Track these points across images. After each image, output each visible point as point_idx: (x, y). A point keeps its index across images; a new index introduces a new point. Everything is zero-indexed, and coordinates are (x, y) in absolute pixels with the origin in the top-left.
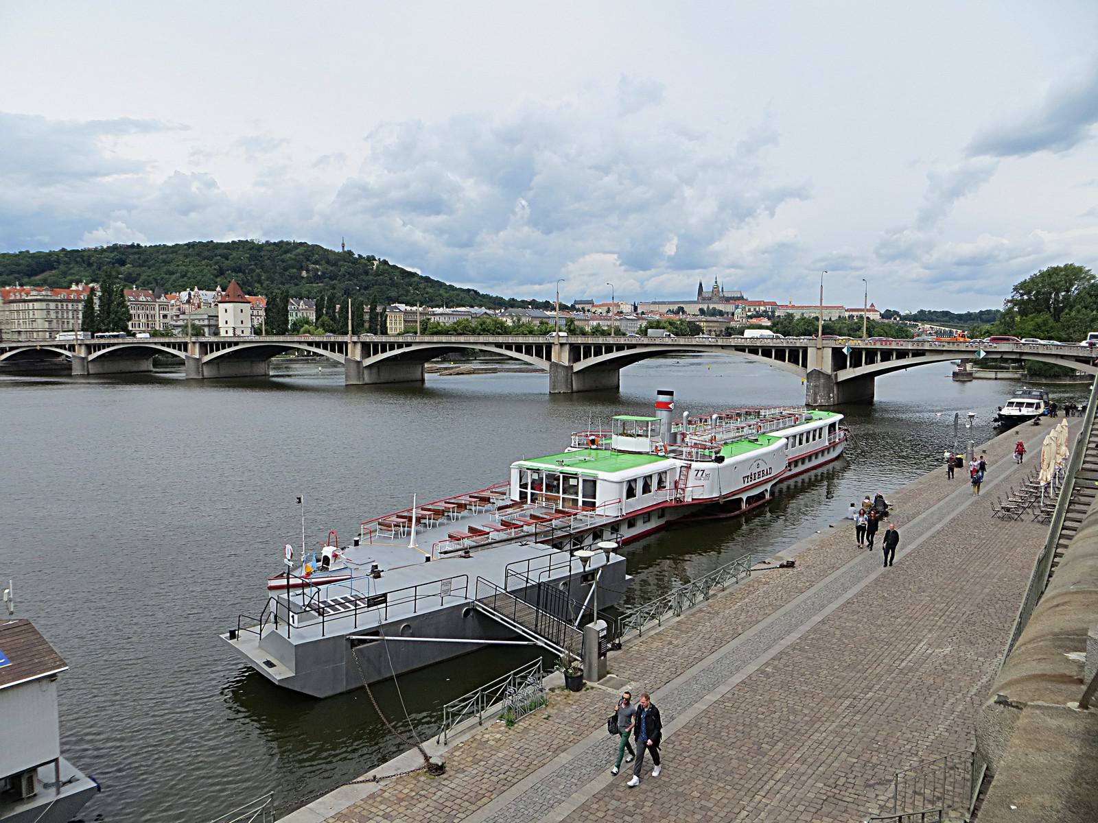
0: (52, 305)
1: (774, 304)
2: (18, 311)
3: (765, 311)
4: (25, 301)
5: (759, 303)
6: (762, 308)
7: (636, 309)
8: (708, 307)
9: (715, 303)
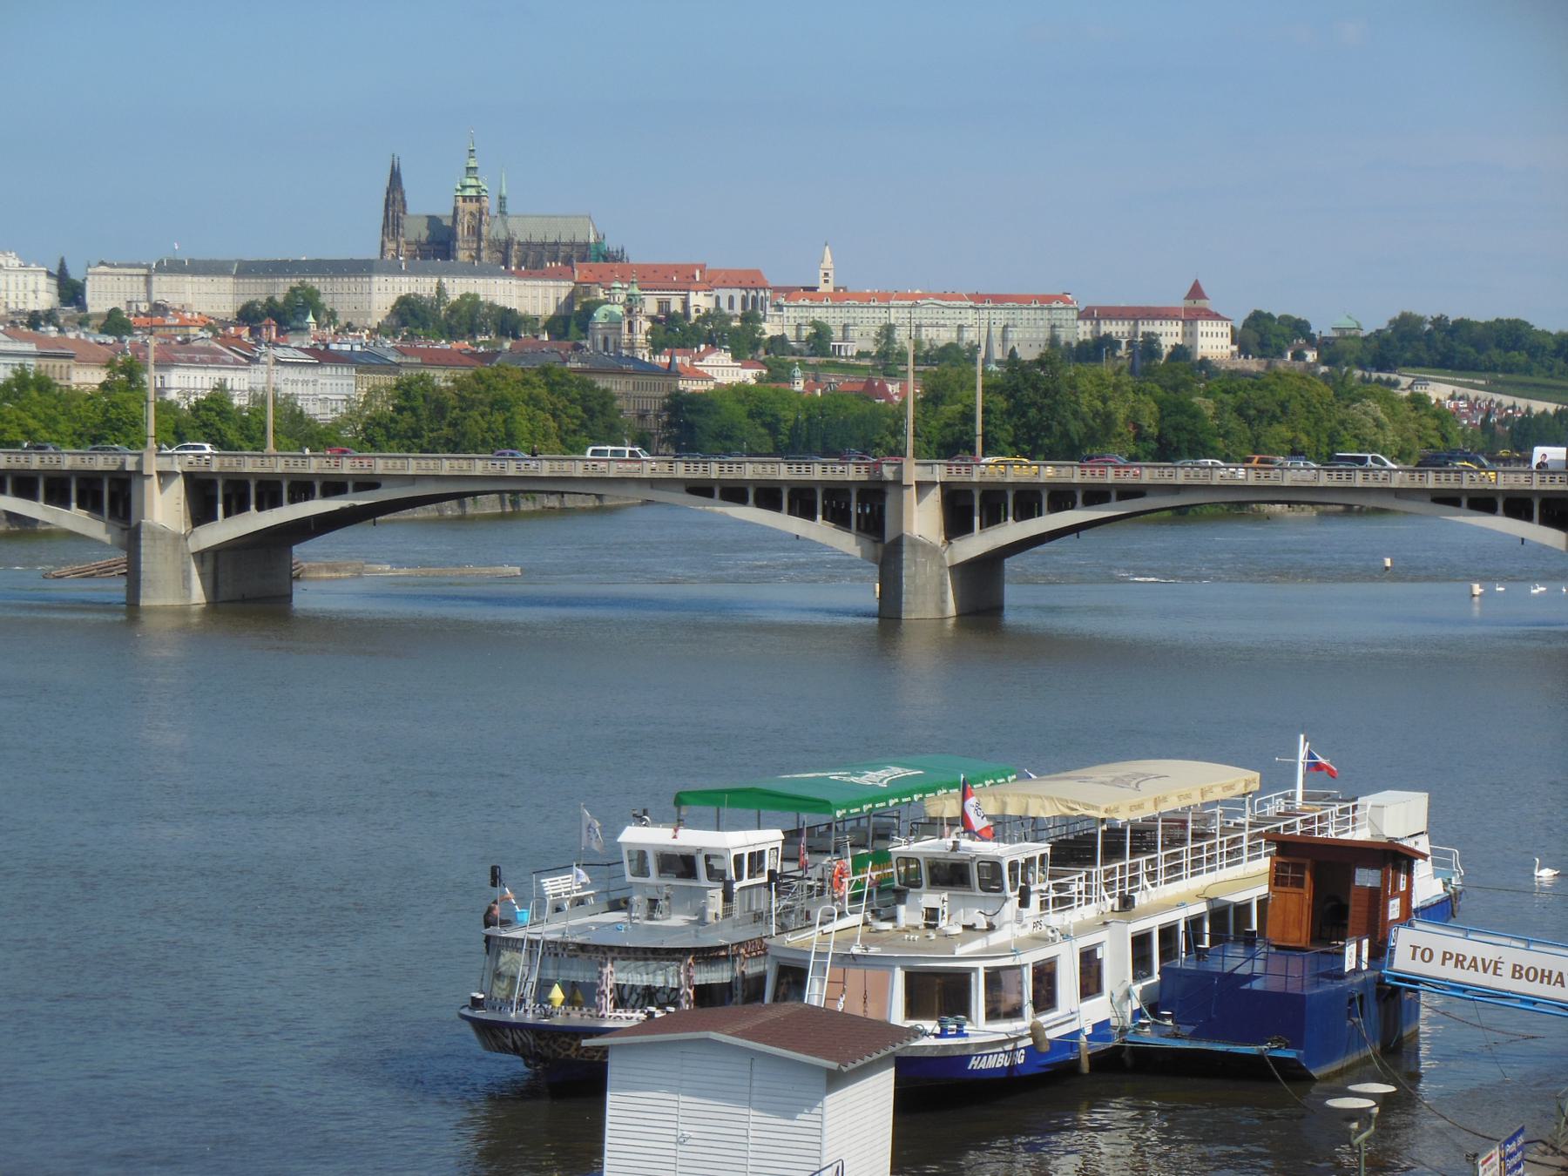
1: (750, 281)
3: (706, 317)
5: (685, 279)
6: (700, 301)
7: (71, 292)
8: (441, 290)
9: (471, 271)
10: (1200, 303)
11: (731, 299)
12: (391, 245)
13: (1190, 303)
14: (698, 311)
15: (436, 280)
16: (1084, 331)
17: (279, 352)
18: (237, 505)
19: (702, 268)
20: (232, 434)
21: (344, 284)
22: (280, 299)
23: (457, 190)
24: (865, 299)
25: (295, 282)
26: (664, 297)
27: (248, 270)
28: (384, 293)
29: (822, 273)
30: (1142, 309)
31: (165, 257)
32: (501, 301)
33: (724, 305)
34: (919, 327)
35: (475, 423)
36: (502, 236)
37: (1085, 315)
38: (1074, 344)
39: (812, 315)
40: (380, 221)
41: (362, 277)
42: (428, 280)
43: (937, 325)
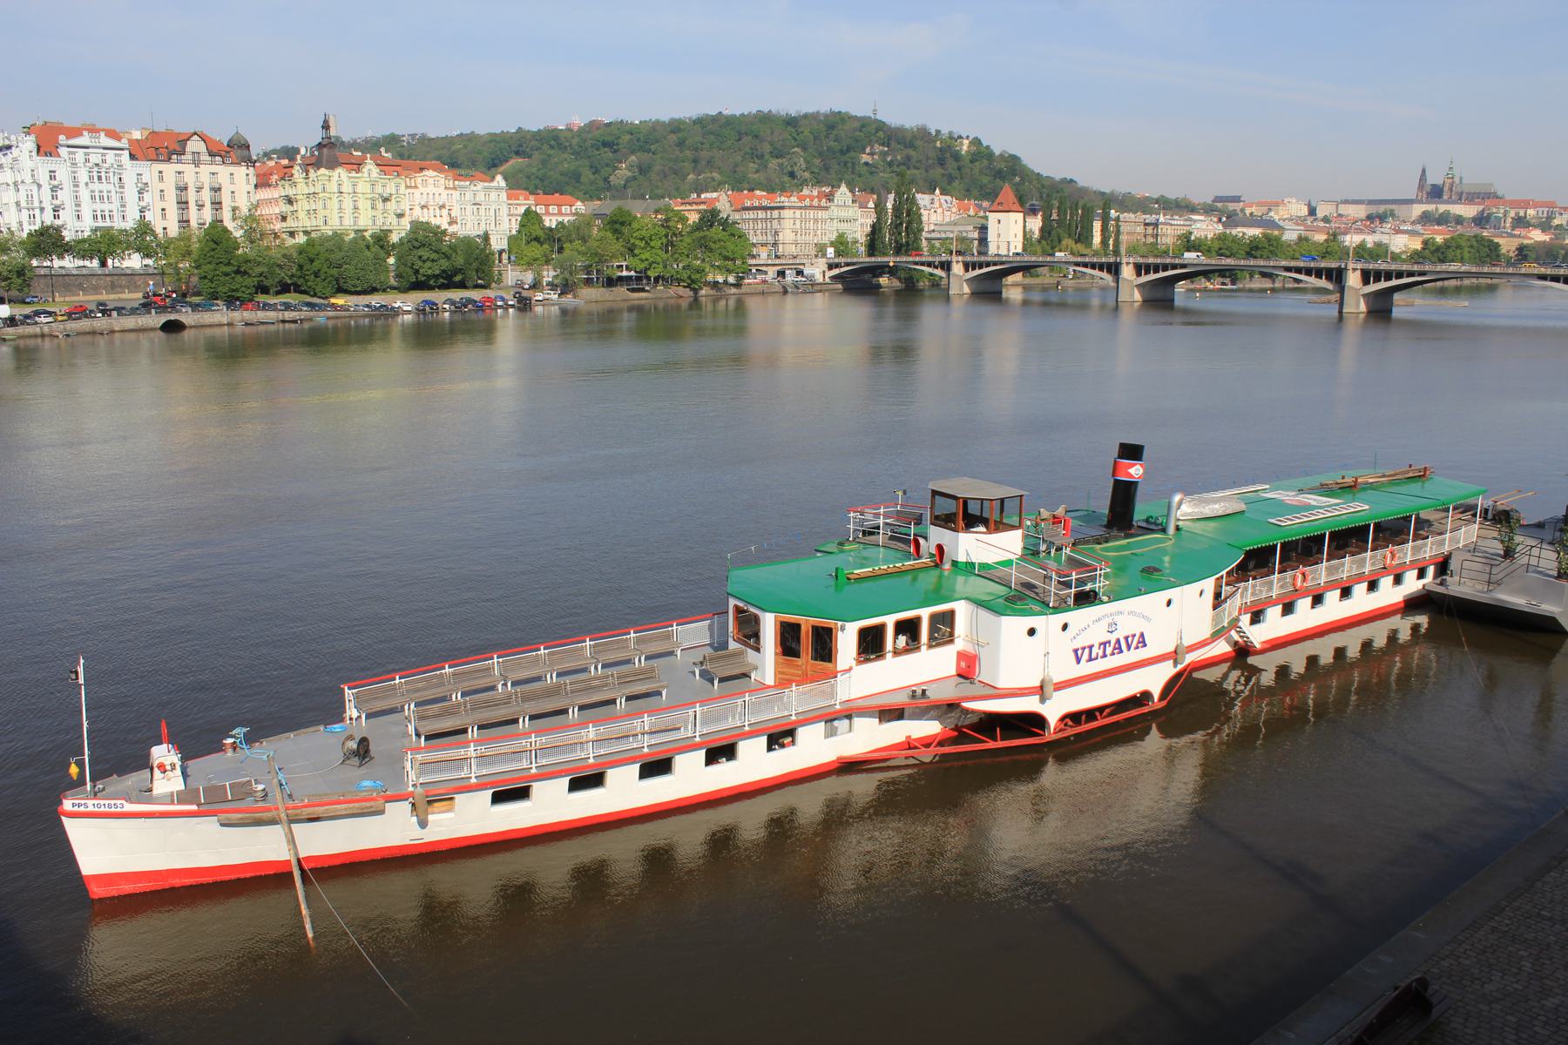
0: (798, 212)
1: (1551, 205)
2: (756, 220)
4: (765, 209)
5: (1526, 204)
7: (1312, 212)
8: (1437, 209)
9: (1447, 202)
17: (1382, 230)
18: (1377, 280)
19: (1533, 201)
20: (1366, 256)
21: (1404, 207)
26: (1517, 210)
27: (1370, 202)
28: (1418, 210)
32: (1458, 213)
35: (1450, 254)
36: (1460, 191)
40: (1417, 186)
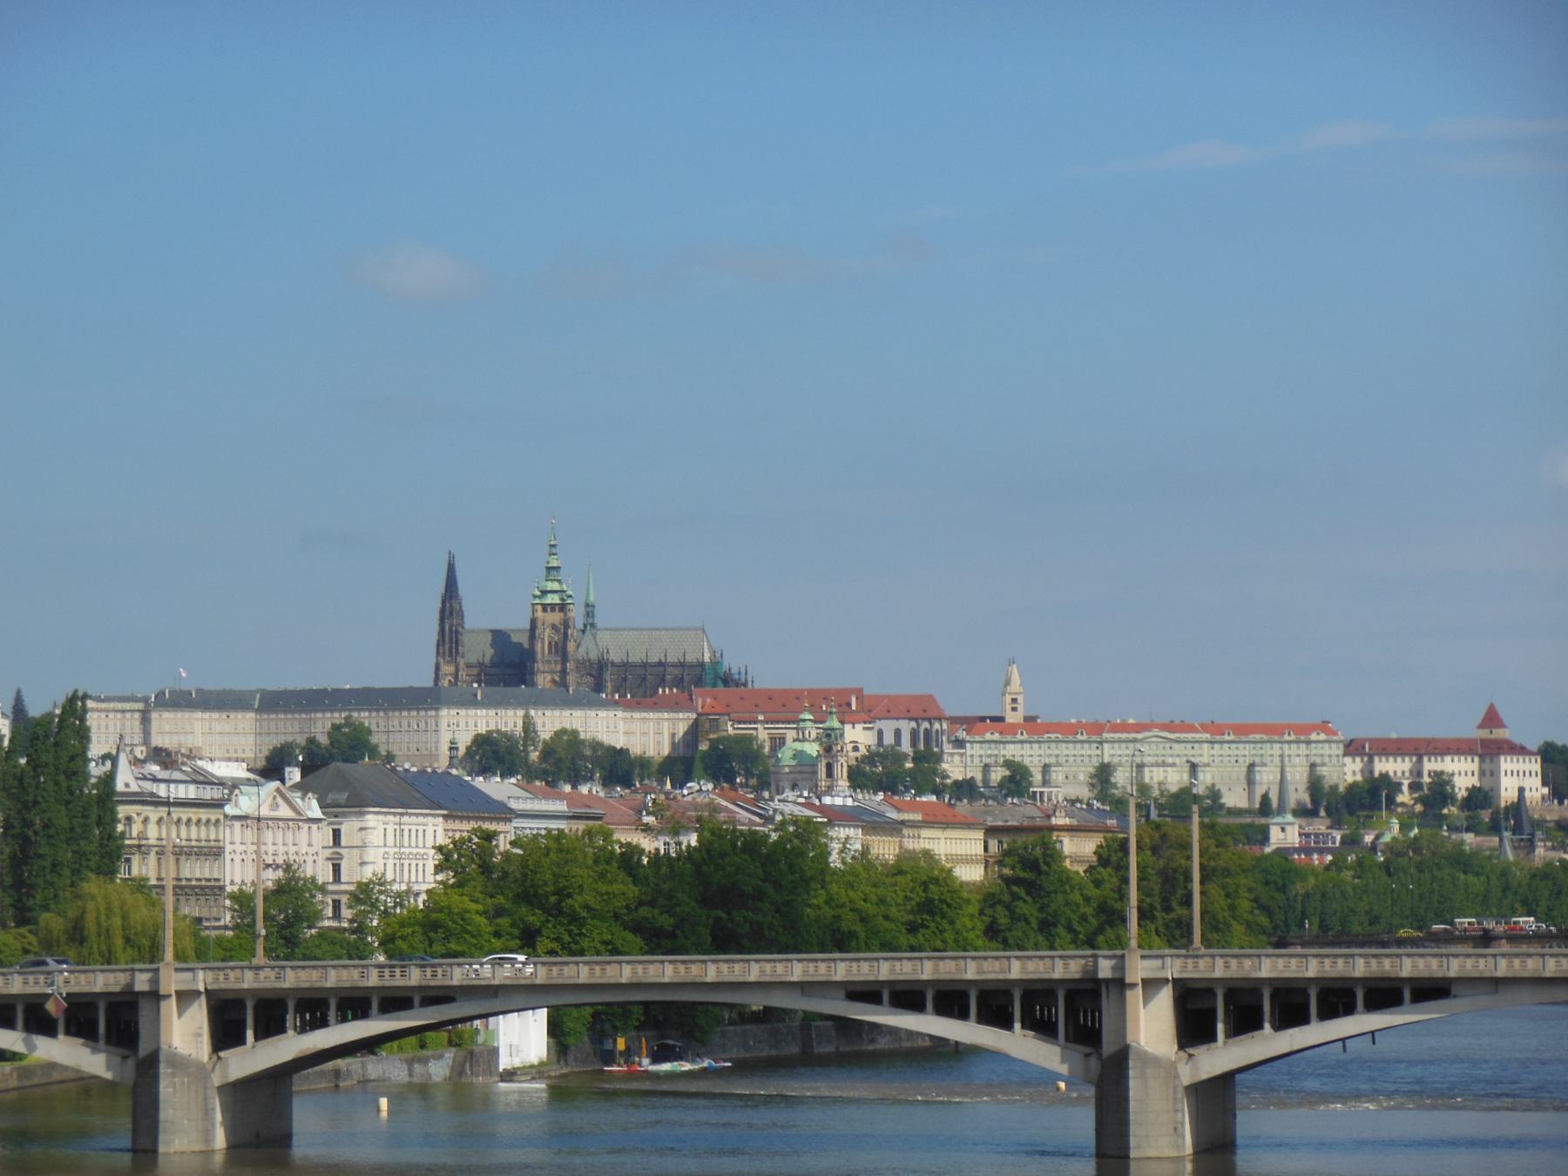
1: (921, 709)
8: (528, 726)
10: (1500, 733)
11: (898, 733)
12: (447, 669)
13: (1484, 734)
14: (856, 749)
15: (521, 713)
16: (1350, 771)
19: (859, 693)
22: (323, 740)
23: (535, 597)
24: (1069, 731)
25: (338, 717)
27: (274, 702)
29: (1008, 698)
30: (1428, 742)
31: (168, 685)
33: (889, 739)
34: (1141, 766)
36: (593, 656)
37: (1353, 748)
38: (1341, 789)
39: (1003, 752)
40: (434, 638)
41: (426, 710)
42: (510, 713)
43: (1164, 764)
